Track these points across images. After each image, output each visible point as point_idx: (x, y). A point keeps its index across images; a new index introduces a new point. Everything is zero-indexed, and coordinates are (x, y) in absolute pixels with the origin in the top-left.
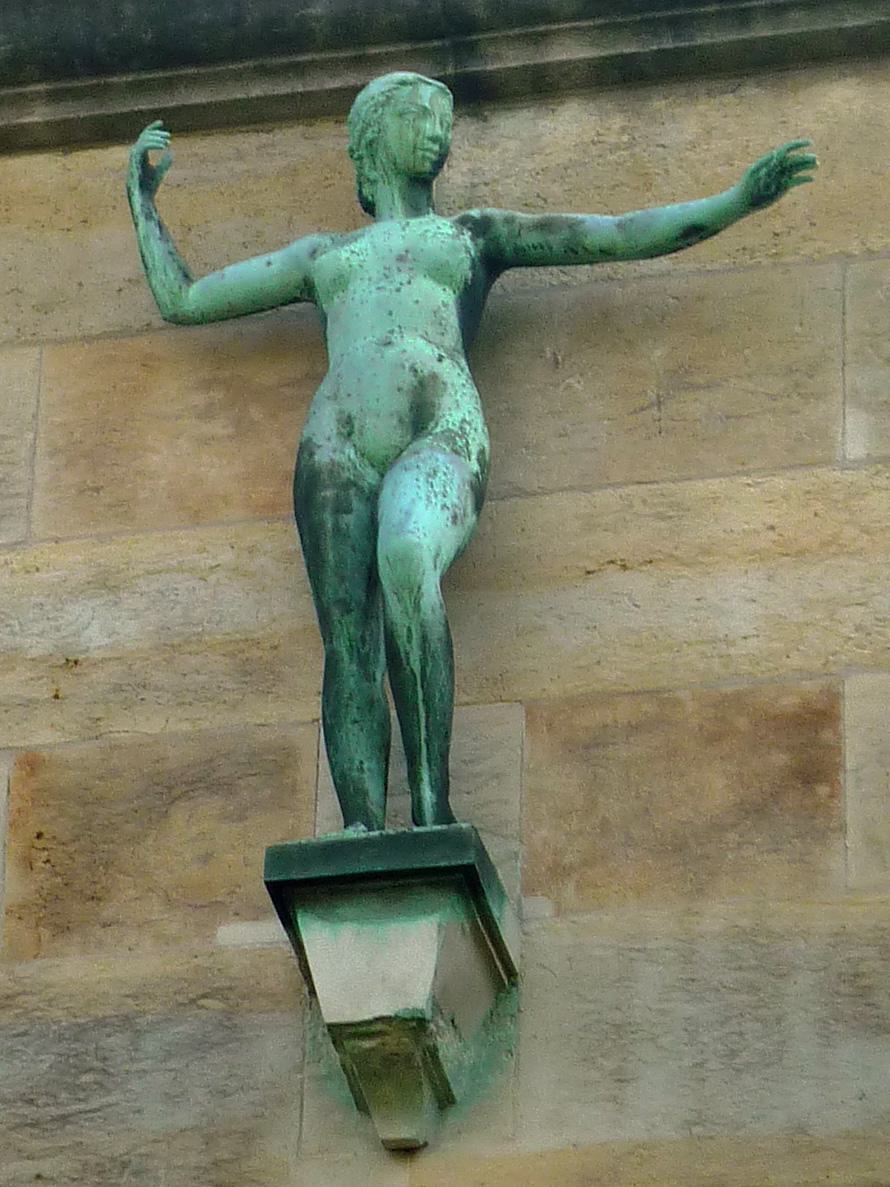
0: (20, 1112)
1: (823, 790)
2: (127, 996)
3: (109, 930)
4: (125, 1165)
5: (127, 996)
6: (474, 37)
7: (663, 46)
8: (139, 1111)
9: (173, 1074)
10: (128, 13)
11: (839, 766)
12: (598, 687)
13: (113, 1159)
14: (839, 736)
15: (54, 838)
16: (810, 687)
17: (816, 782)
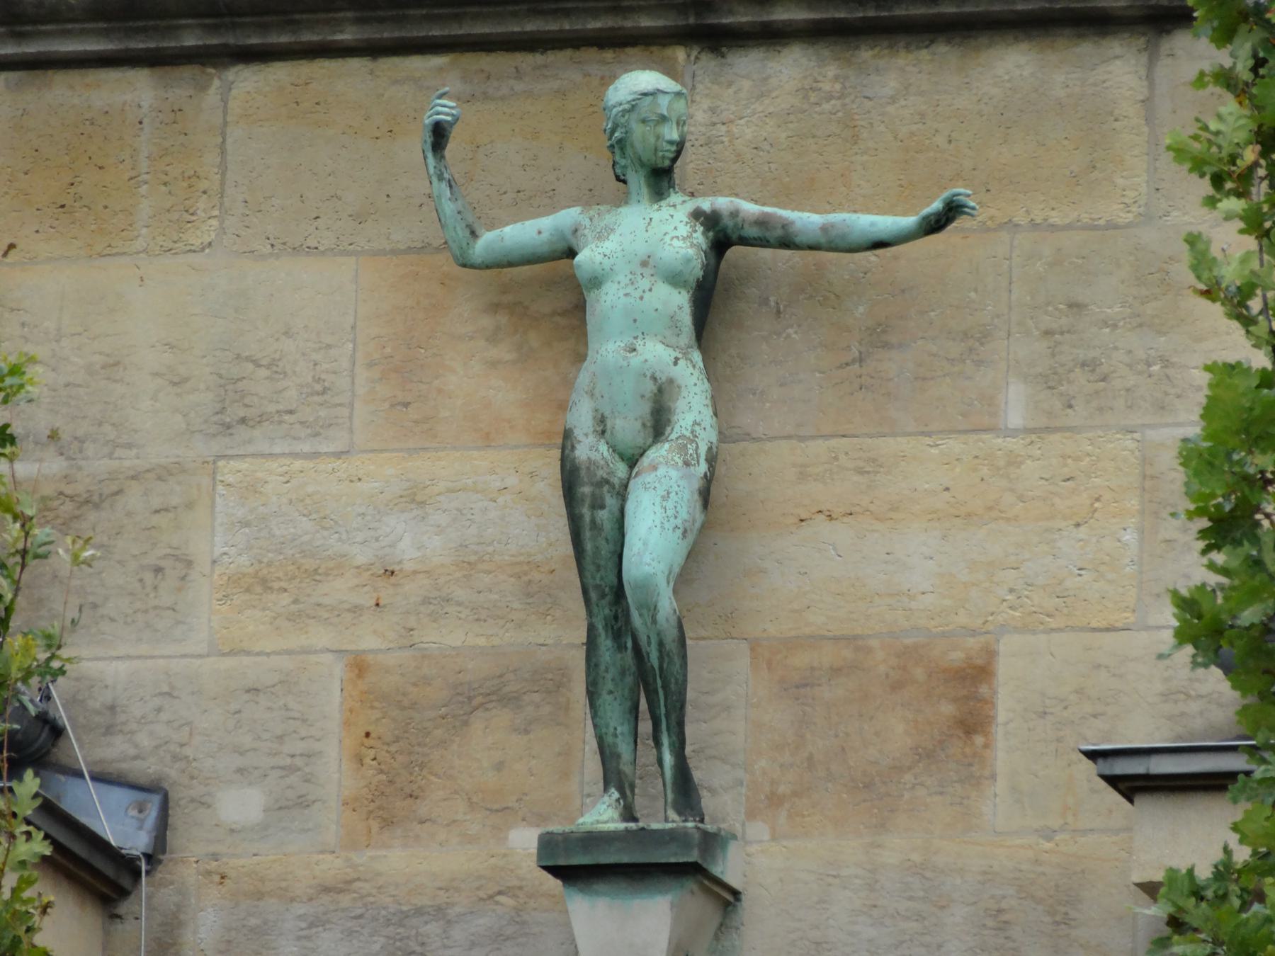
1: (979, 740)
14: (995, 693)
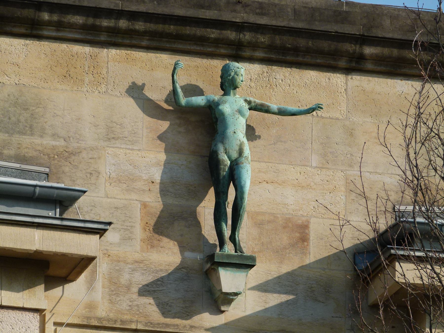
0: (146, 288)
1: (306, 244)
2: (167, 265)
3: (162, 248)
4: (167, 304)
5: (167, 265)
6: (299, 53)
7: (280, 57)
8: (169, 292)
9: (176, 285)
10: (332, 47)
11: (309, 239)
12: (262, 211)
13: (165, 302)
14: (309, 232)
15: (150, 224)
16: (304, 219)
17: (305, 242)
